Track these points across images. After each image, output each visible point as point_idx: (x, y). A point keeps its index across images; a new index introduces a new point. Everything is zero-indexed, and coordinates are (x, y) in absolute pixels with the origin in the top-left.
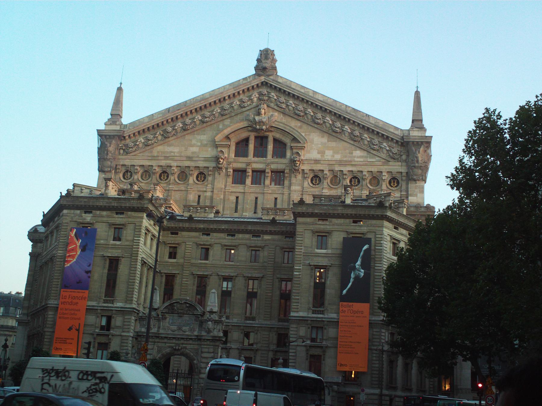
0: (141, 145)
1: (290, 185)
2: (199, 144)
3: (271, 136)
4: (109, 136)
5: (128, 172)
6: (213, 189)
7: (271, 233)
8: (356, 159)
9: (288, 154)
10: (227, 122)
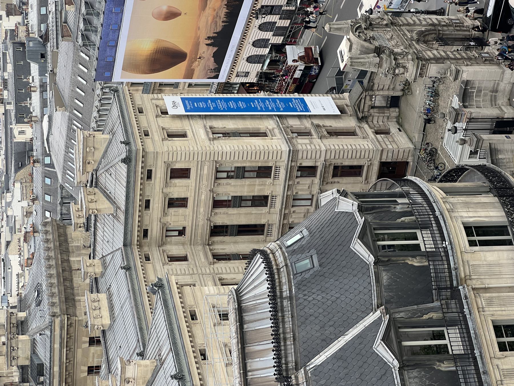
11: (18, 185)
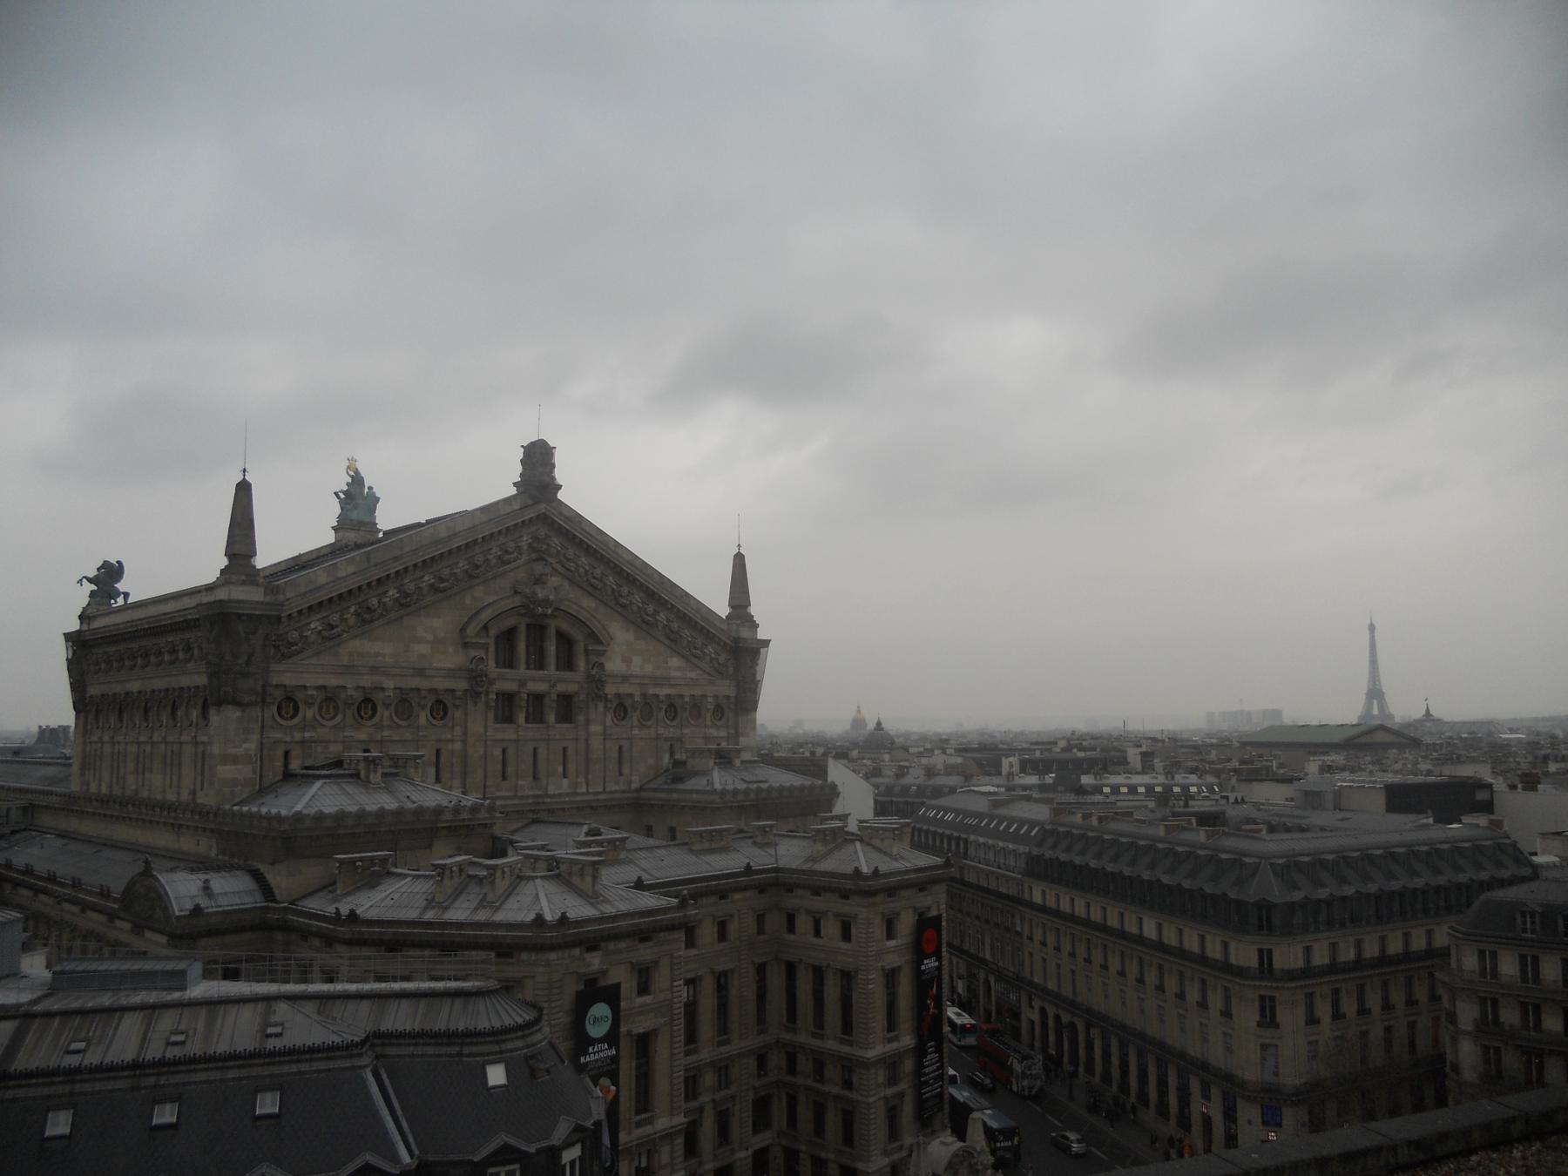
0: (313, 637)
1: (588, 722)
2: (430, 637)
3: (553, 625)
4: (249, 616)
5: (289, 703)
6: (465, 733)
7: (745, 888)
8: (674, 674)
9: (581, 664)
10: (479, 591)
11: (959, 760)
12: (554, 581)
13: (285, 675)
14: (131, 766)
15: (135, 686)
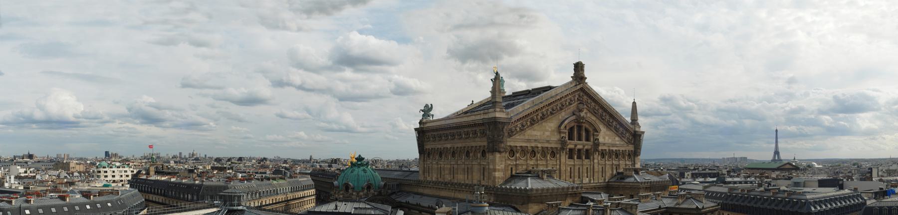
5: (512, 152)
10: (563, 114)
12: (585, 111)
13: (511, 142)
14: (447, 172)
15: (449, 146)
